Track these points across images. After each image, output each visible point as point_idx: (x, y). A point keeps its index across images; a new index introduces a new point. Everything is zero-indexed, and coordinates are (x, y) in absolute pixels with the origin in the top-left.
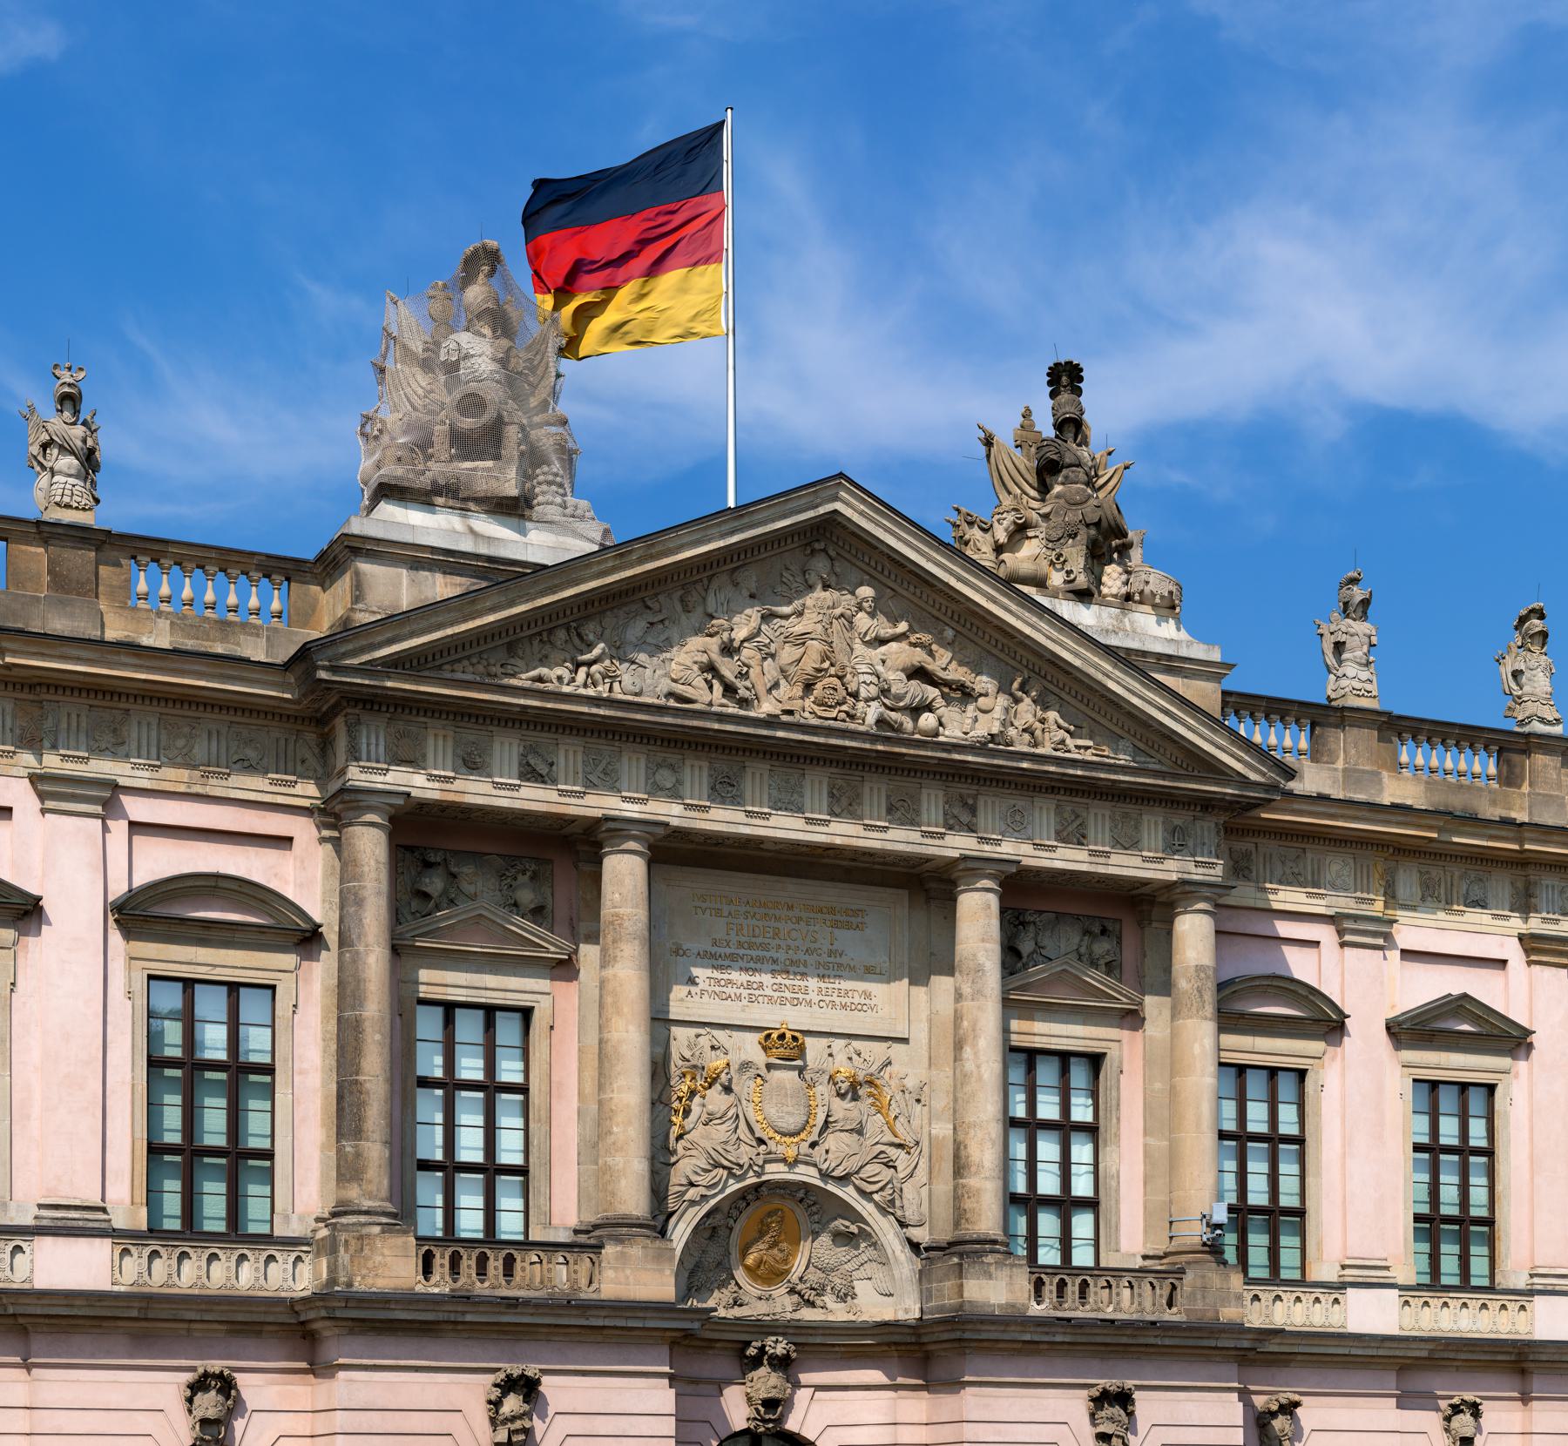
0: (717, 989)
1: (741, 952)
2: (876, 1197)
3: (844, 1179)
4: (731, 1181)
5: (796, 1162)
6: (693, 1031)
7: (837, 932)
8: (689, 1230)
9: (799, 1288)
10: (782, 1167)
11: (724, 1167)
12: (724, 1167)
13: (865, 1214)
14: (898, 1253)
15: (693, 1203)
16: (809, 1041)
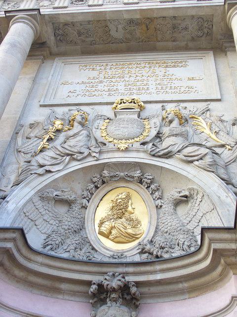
0: (87, 94)
1: (105, 80)
2: (196, 163)
3: (168, 155)
4: (75, 163)
5: (127, 150)
6: (66, 109)
7: (168, 69)
8: (33, 192)
9: (148, 247)
10: (117, 155)
11: (68, 155)
12: (68, 155)
13: (190, 176)
14: (223, 198)
15: (40, 175)
16: (148, 106)
